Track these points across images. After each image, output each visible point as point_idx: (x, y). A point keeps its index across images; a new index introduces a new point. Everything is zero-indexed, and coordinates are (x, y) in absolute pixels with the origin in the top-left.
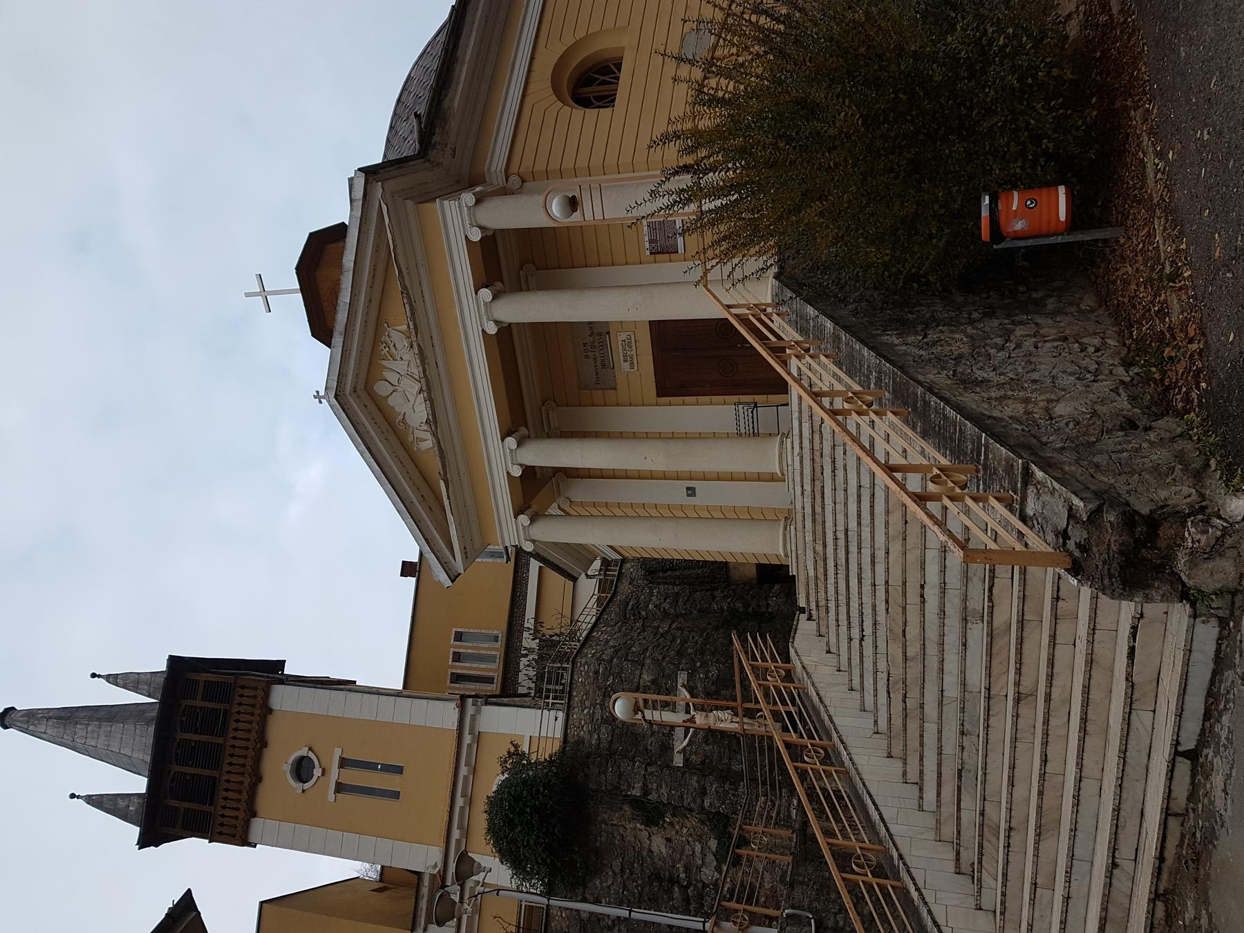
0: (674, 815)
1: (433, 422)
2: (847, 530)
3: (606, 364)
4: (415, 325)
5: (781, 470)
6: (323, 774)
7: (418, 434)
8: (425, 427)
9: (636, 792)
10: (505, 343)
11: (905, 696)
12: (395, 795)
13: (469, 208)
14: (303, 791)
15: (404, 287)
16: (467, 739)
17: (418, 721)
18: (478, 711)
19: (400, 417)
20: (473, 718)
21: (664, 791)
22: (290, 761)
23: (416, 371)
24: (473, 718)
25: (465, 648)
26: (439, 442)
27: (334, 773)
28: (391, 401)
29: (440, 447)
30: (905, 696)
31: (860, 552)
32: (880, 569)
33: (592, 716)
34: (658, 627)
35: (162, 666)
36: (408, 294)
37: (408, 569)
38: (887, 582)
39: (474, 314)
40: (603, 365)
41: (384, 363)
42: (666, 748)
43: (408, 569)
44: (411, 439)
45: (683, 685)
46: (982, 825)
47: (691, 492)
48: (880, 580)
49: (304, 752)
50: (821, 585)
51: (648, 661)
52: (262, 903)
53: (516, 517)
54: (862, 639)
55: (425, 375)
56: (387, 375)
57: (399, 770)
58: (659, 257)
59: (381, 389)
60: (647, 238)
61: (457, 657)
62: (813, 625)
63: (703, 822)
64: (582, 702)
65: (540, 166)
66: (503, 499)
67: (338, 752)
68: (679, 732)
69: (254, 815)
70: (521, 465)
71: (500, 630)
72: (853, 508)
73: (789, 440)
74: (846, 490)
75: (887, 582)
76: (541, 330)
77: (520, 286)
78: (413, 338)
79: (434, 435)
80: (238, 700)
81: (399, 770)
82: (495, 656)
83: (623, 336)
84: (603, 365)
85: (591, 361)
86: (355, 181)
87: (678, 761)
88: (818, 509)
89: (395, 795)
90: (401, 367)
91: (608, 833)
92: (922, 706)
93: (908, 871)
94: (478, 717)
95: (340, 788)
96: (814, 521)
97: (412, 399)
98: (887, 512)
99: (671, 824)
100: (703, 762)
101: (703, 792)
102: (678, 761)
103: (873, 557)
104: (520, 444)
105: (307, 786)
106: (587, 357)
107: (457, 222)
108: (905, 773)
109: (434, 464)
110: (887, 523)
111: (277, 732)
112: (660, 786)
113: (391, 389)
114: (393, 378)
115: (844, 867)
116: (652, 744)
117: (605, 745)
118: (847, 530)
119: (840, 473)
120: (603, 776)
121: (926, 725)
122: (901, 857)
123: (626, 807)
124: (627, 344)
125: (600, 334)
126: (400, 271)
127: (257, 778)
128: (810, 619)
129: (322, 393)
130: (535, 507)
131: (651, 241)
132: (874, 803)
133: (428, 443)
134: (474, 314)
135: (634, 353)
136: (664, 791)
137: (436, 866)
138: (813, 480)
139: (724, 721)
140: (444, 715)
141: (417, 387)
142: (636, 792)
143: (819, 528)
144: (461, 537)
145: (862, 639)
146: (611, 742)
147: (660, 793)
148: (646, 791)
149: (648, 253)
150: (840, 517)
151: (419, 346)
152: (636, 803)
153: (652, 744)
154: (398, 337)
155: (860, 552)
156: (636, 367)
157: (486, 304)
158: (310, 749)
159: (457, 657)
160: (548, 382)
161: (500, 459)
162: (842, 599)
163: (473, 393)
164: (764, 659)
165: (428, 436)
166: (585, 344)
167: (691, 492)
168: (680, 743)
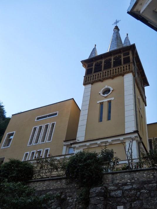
6: (105, 97)
12: (101, 120)
14: (100, 94)
16: (121, 138)
22: (108, 87)
27: (106, 100)
33: (126, 184)
35: (132, 43)
49: (111, 89)
52: (73, 99)
57: (109, 118)
69: (92, 84)
80: (125, 66)
81: (109, 118)
89: (101, 120)
91: (72, 203)
105: (102, 94)
111: (117, 80)
127: (101, 81)
146: (113, 197)
158: (113, 91)
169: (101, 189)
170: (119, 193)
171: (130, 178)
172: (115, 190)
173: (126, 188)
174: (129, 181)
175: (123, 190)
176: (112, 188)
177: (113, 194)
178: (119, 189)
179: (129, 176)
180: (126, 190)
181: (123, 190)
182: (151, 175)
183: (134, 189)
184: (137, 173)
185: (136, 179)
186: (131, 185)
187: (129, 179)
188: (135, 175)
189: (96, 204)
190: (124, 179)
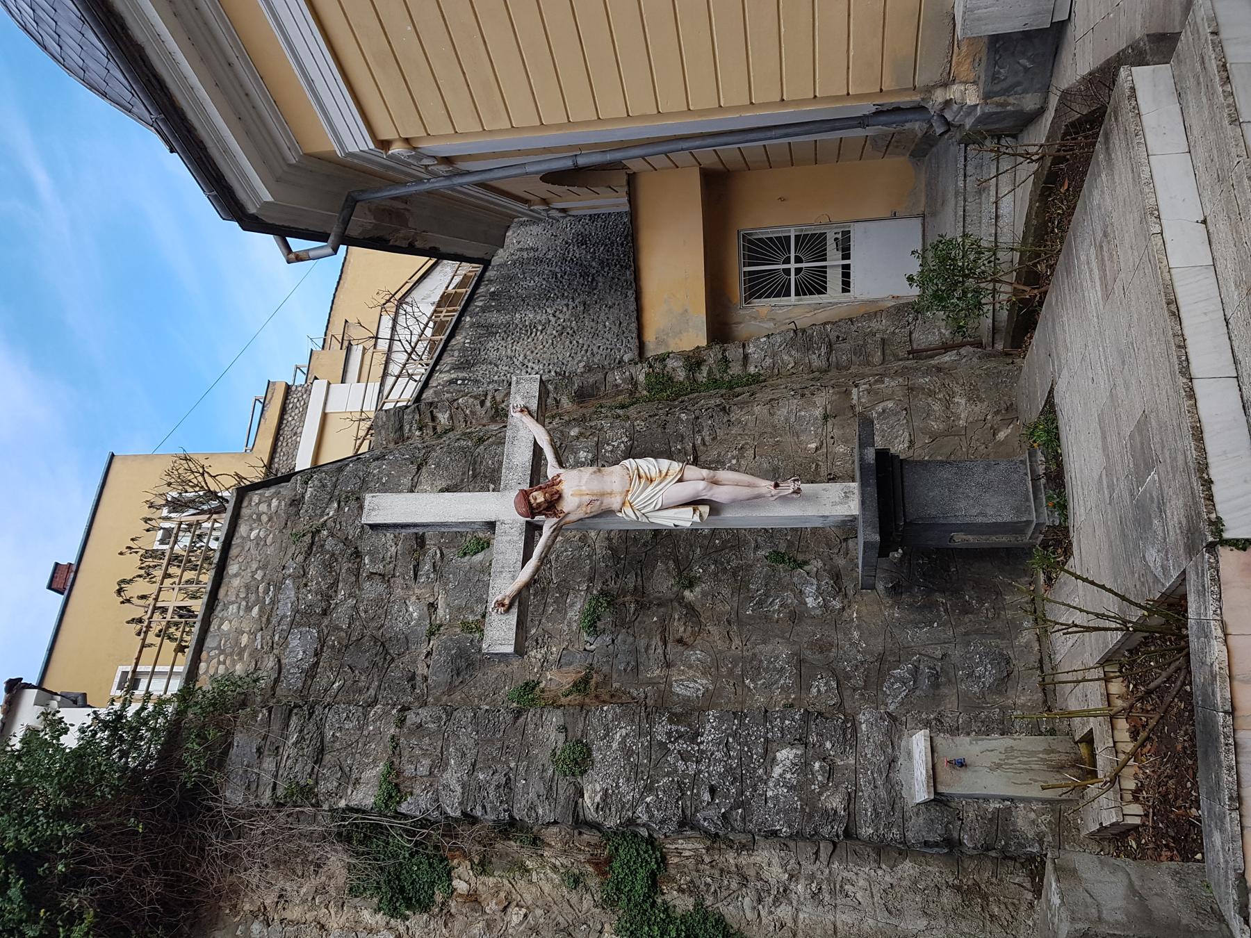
0: (483, 867)
9: (365, 795)
21: (452, 777)
45: (525, 410)
63: (576, 881)
68: (508, 544)
99: (473, 899)
100: (581, 685)
101: (579, 759)
112: (441, 763)
117: (294, 679)
120: (269, 764)
123: (337, 862)
136: (452, 777)
139: (654, 493)
142: (365, 795)
146: (311, 673)
147: (442, 788)
148: (394, 789)
152: (358, 832)
171: (244, 603)
184: (233, 568)
185: (259, 576)
188: (236, 582)
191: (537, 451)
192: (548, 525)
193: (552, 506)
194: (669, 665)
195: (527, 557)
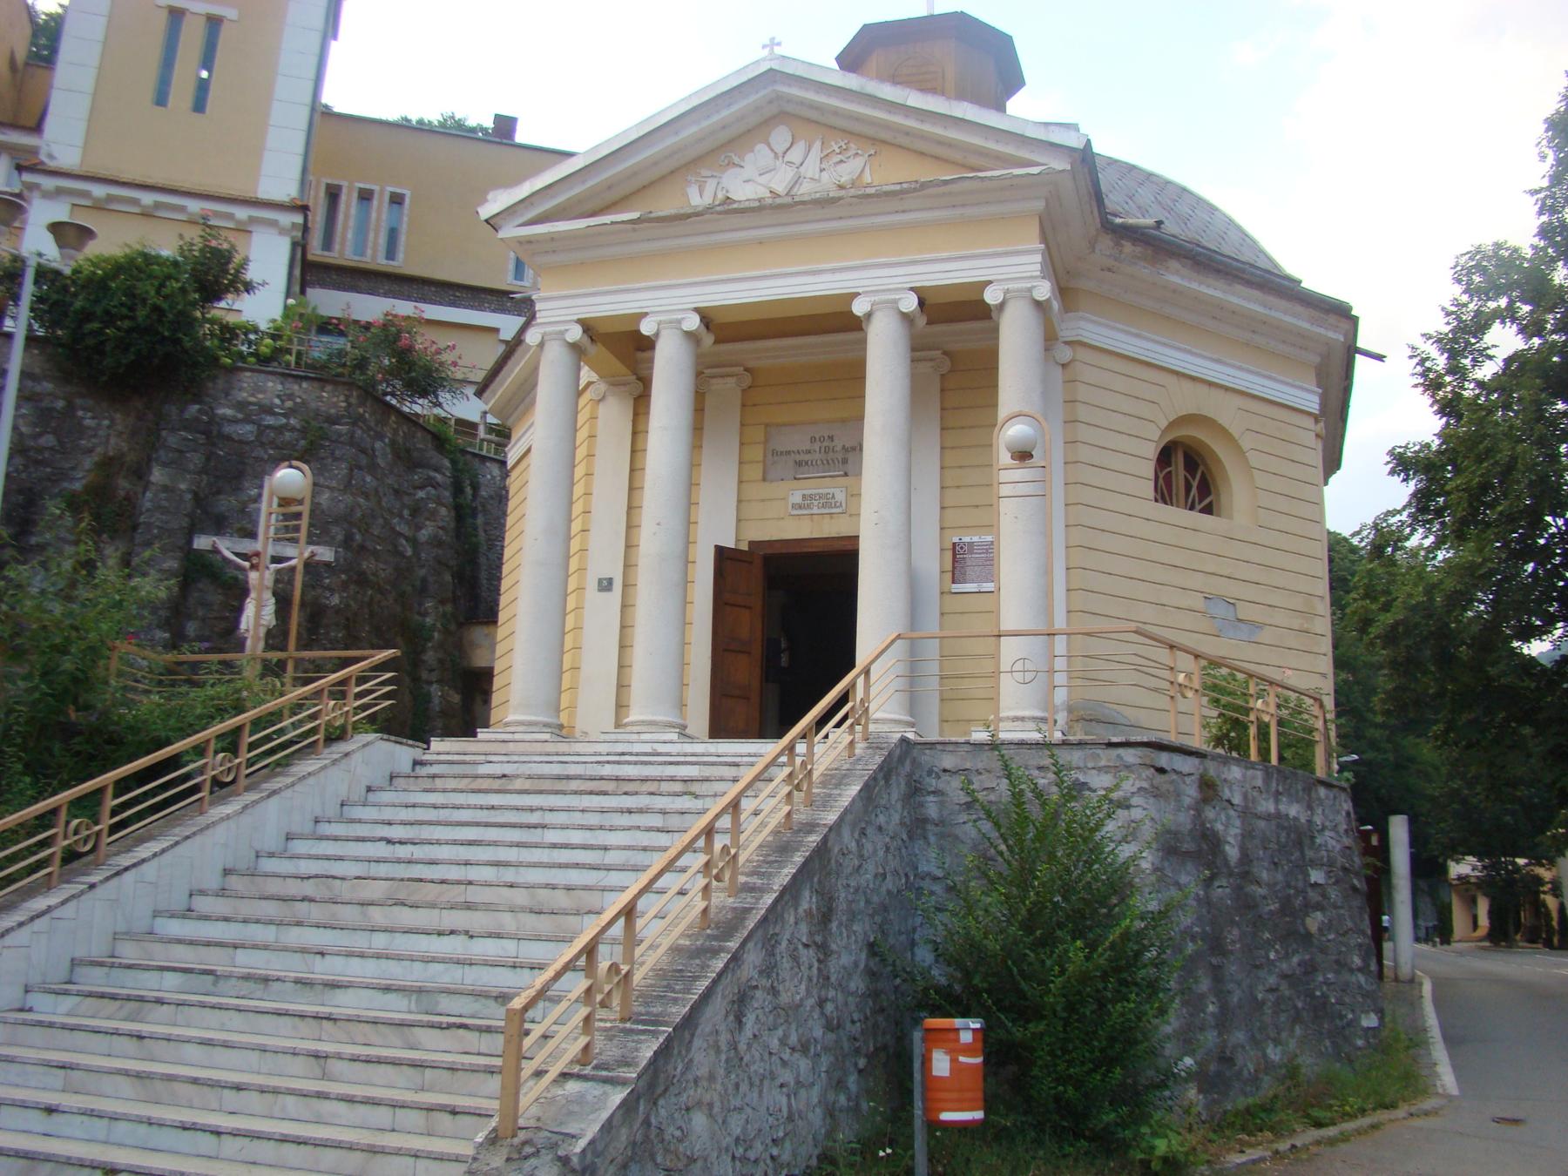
1: (728, 209)
2: (544, 827)
3: (801, 466)
4: (869, 196)
5: (633, 724)
7: (710, 186)
8: (720, 196)
10: (837, 322)
11: (312, 900)
12: (161, 99)
13: (1030, 290)
15: (924, 186)
17: (273, 139)
18: (282, 231)
19: (736, 160)
20: (273, 224)
23: (805, 190)
24: (273, 224)
25: (380, 210)
26: (697, 214)
28: (761, 148)
29: (689, 216)
30: (312, 900)
31: (512, 845)
32: (488, 874)
33: (268, 410)
34: (401, 516)
36: (915, 190)
37: (505, 126)
38: (470, 883)
39: (882, 284)
40: (799, 464)
41: (818, 144)
42: (219, 525)
43: (505, 126)
44: (705, 172)
45: (313, 554)
46: (141, 999)
47: (606, 585)
48: (473, 873)
50: (463, 784)
51: (348, 499)
53: (579, 321)
54: (389, 841)
55: (797, 203)
56: (800, 148)
57: (199, 106)
58: (949, 555)
59: (780, 137)
60: (975, 539)
61: (365, 196)
62: (406, 767)
64: (291, 397)
65: (1083, 392)
66: (609, 303)
67: (229, 13)
68: (246, 546)
70: (657, 335)
71: (402, 264)
72: (576, 837)
73: (674, 737)
74: (601, 828)
75: (470, 883)
76: (853, 376)
77: (918, 349)
78: (853, 192)
79: (709, 210)
81: (199, 106)
82: (363, 254)
83: (840, 496)
84: (799, 464)
85: (807, 446)
86: (1073, 134)
87: (202, 542)
88: (574, 785)
89: (161, 99)
90: (811, 168)
92: (299, 924)
93: (73, 897)
94: (274, 231)
95: (176, 14)
96: (559, 778)
97: (762, 180)
98: (569, 889)
102: (202, 542)
103: (506, 864)
104: (689, 335)
106: (813, 440)
107: (1011, 272)
108: (202, 893)
109: (666, 206)
110: (554, 887)
113: (780, 149)
114: (795, 155)
115: (78, 805)
116: (226, 503)
118: (544, 827)
119: (625, 820)
121: (273, 928)
122: (92, 886)
124: (828, 501)
125: (845, 461)
126: (946, 182)
128: (416, 763)
129: (777, 50)
130: (594, 350)
131: (971, 544)
132: (163, 851)
133: (697, 198)
134: (882, 284)
135: (815, 511)
137: (51, 156)
138: (617, 779)
139: (257, 615)
140: (279, 179)
141: (781, 188)
143: (547, 785)
144: (552, 238)
145: (389, 841)
146: (229, 438)
149: (956, 540)
150: (561, 818)
151: (840, 199)
153: (226, 503)
154: (852, 168)
155: (512, 845)
156: (790, 517)
157: (895, 302)
159: (365, 196)
160: (777, 373)
161: (668, 305)
162: (443, 815)
163: (767, 272)
164: (359, 696)
165: (707, 200)
166: (831, 438)
167: (606, 585)
168: (227, 547)
169: (199, 411)
170: (246, 431)
172: (235, 421)
173: (270, 420)
174: (277, 401)
175: (259, 425)
176: (229, 412)
177: (228, 429)
178: (247, 420)
179: (280, 387)
180: (269, 427)
181: (259, 425)
182: (342, 398)
183: (293, 429)
184: (305, 385)
186: (284, 415)
187: (278, 396)
188: (296, 387)
189: (181, 452)
190: (264, 392)
191: (290, 559)
192: (247, 564)
193: (253, 567)
194: (203, 620)
195: (237, 554)
